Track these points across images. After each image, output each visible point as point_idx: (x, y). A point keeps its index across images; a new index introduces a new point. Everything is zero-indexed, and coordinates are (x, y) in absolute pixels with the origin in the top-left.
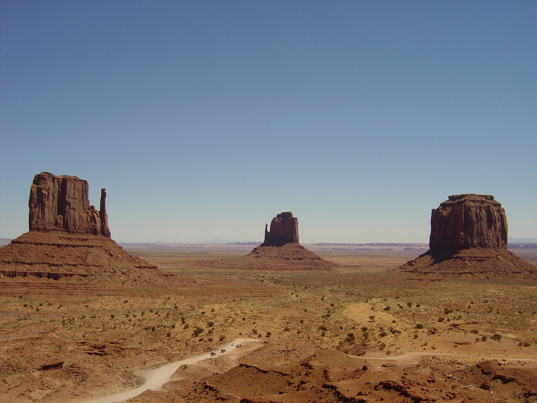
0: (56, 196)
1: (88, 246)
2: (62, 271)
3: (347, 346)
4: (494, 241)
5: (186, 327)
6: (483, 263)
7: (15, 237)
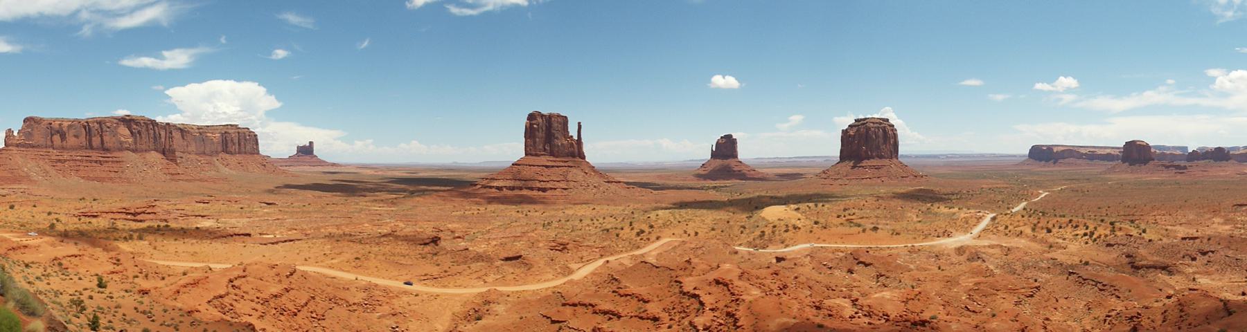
0: (544, 129)
1: (569, 166)
2: (549, 185)
3: (758, 242)
5: (632, 229)
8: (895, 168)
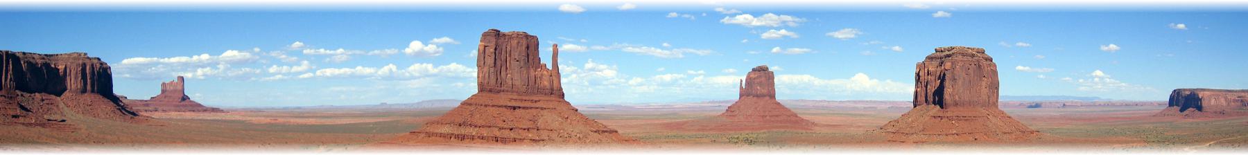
6: (972, 123)
7: (465, 98)
8: (994, 120)
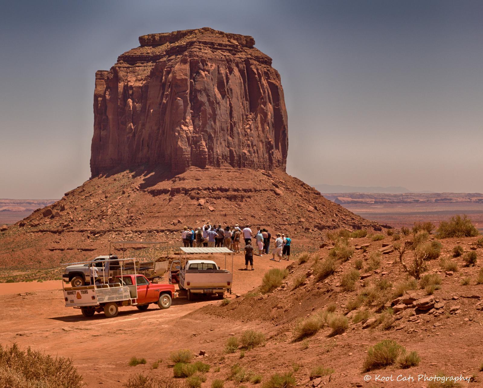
4: (260, 152)
6: (242, 204)
